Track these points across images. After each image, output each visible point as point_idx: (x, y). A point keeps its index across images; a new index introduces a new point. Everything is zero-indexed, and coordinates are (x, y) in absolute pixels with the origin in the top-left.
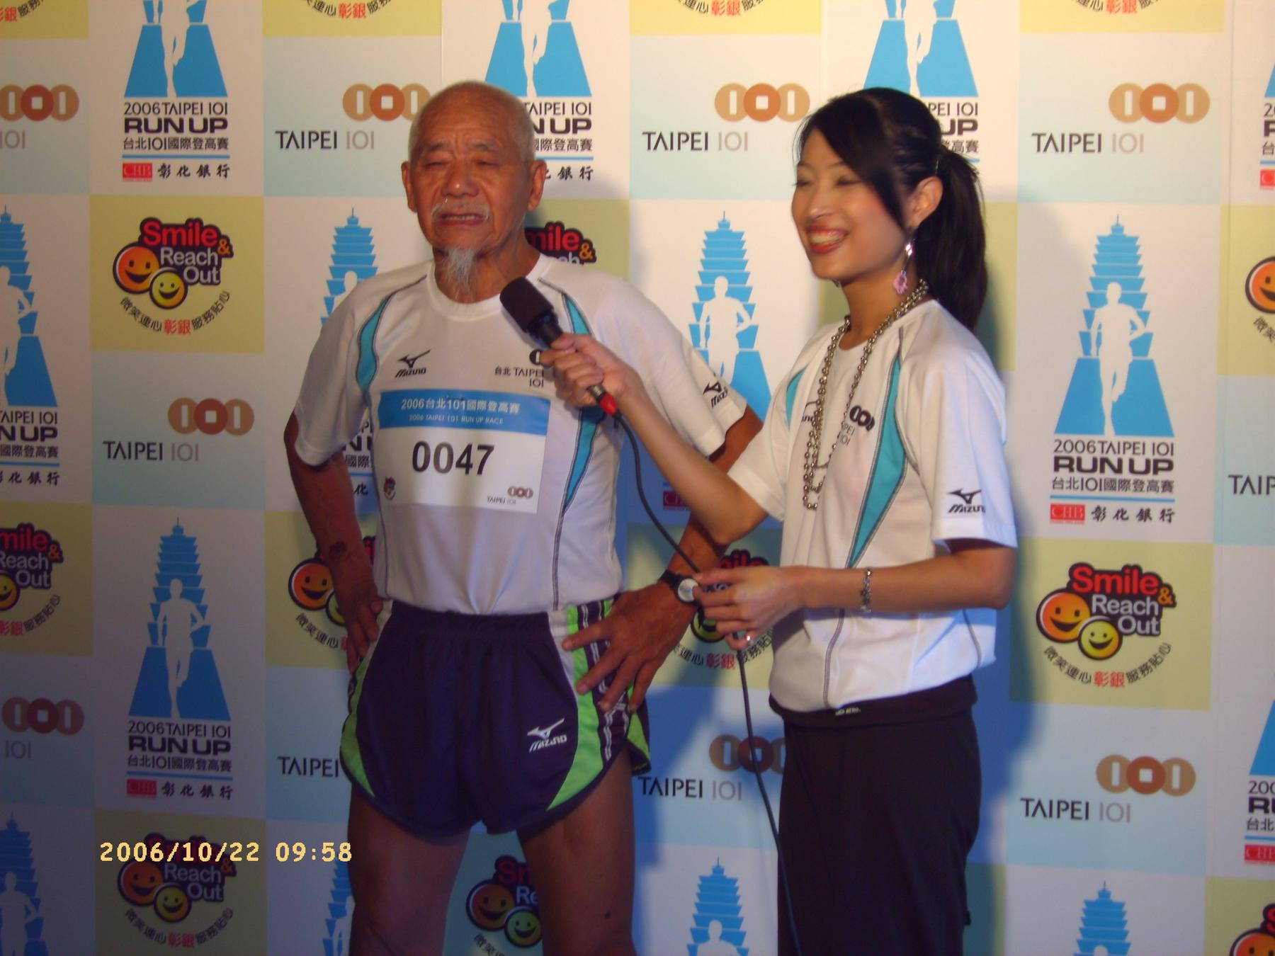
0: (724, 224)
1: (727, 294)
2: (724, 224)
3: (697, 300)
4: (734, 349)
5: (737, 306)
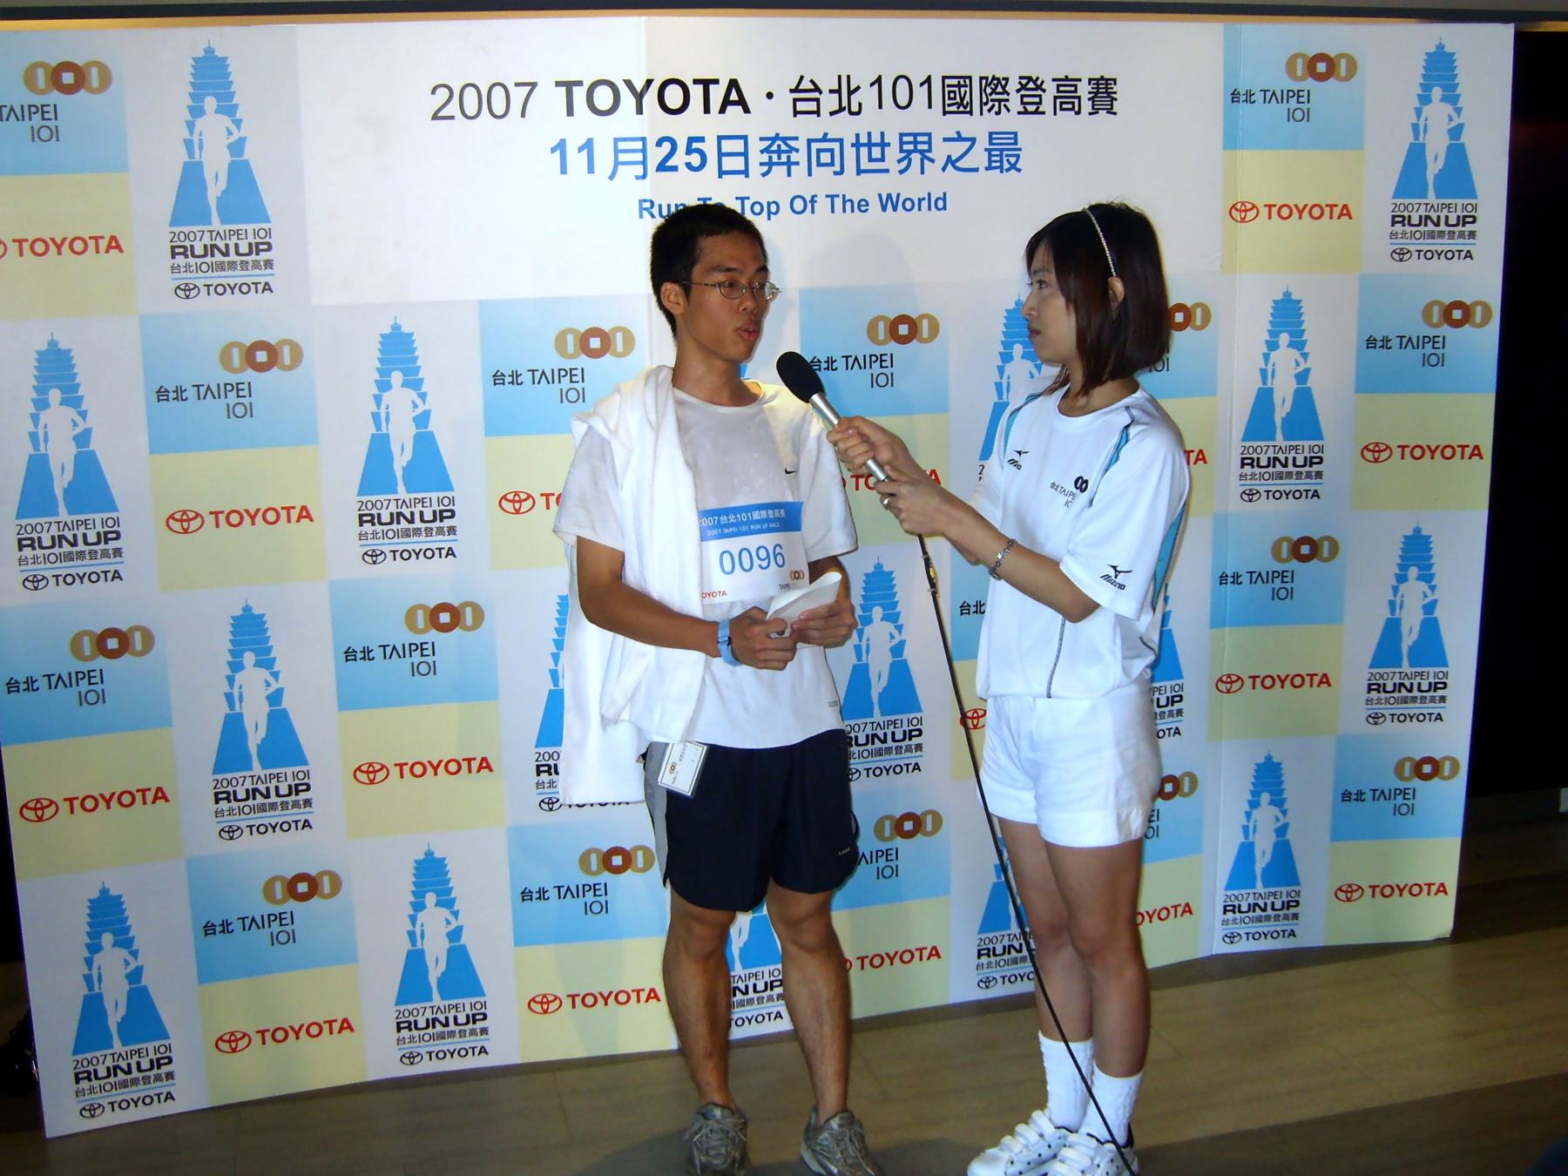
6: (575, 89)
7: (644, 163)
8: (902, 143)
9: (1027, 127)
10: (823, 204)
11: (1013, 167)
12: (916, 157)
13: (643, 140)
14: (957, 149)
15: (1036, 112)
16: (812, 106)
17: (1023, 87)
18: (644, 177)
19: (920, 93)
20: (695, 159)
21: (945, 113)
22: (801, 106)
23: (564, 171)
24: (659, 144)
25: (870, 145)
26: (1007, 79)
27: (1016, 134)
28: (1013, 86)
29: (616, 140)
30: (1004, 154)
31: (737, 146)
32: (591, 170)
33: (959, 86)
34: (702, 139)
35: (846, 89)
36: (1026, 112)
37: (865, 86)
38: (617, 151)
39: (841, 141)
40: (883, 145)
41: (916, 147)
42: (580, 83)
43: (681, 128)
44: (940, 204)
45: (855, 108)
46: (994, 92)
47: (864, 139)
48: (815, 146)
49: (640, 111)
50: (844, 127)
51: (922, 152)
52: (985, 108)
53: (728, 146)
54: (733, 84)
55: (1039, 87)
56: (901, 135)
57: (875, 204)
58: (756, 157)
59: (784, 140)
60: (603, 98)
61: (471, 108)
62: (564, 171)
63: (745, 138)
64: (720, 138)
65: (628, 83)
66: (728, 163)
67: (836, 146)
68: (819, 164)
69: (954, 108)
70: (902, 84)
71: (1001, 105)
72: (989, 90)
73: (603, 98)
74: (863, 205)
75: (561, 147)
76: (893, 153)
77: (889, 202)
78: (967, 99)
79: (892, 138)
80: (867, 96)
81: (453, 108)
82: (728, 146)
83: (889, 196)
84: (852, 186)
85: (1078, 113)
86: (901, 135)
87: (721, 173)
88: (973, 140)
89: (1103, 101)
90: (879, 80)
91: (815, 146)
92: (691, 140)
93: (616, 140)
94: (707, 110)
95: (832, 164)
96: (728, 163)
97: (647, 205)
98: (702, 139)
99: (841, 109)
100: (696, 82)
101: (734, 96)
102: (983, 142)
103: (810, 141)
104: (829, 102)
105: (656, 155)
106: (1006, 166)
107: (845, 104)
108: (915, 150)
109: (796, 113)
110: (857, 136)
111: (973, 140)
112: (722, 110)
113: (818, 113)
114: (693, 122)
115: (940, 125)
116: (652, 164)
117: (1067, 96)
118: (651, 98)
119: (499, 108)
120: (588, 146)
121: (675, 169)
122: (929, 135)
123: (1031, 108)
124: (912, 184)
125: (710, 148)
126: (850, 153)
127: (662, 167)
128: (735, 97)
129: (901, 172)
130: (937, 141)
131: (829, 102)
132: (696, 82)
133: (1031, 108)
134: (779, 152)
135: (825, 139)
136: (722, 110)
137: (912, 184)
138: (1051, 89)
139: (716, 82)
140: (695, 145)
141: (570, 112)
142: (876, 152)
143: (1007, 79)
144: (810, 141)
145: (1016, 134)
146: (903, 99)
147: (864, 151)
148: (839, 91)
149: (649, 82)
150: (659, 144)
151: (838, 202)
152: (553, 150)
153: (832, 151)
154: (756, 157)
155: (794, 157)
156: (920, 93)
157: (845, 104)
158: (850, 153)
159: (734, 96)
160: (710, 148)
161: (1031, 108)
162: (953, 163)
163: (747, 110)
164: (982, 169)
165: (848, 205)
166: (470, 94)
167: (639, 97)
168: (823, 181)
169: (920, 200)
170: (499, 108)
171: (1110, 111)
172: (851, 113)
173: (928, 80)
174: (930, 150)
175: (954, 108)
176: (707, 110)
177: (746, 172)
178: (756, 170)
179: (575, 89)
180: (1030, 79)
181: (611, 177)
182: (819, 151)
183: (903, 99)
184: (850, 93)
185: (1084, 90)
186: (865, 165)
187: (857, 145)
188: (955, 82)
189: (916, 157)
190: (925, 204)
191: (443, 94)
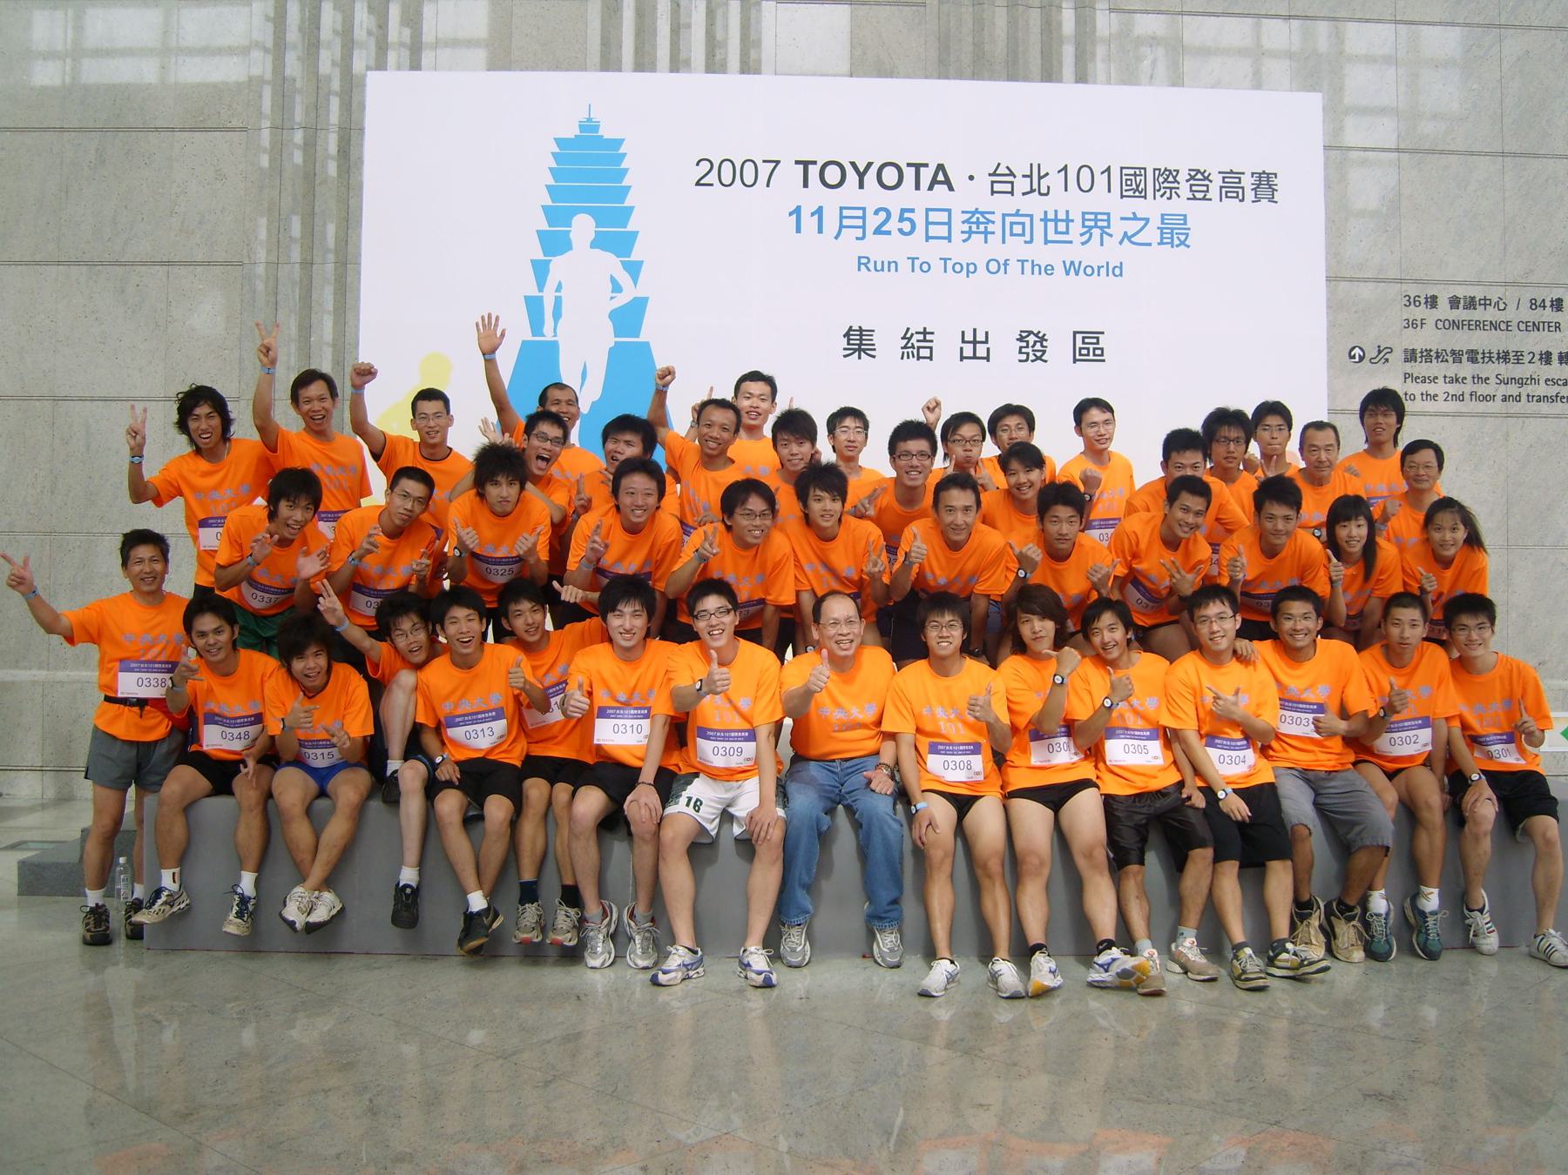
0: (589, 126)
1: (595, 244)
2: (589, 126)
3: (540, 256)
4: (607, 338)
5: (610, 263)
7: (863, 227)
8: (1084, 220)
9: (1195, 210)
10: (1014, 267)
11: (1182, 243)
12: (1096, 232)
13: (864, 209)
14: (1132, 227)
15: (1204, 198)
16: (1008, 187)
17: (1192, 178)
18: (863, 238)
19: (1101, 180)
20: (906, 226)
22: (997, 187)
23: (798, 231)
24: (876, 213)
25: (1056, 220)
30: (1174, 233)
31: (944, 217)
32: (820, 231)
34: (912, 211)
35: (1036, 176)
36: (1195, 198)
38: (842, 217)
39: (1031, 216)
40: (1068, 221)
41: (1096, 224)
42: (815, 163)
46: (1166, 180)
47: (1051, 216)
48: (1008, 220)
49: (861, 186)
50: (1035, 205)
53: (933, 217)
54: (941, 167)
55: (1206, 178)
57: (1059, 269)
58: (958, 226)
59: (982, 214)
60: (833, 175)
61: (727, 179)
62: (798, 231)
63: (949, 211)
64: (928, 210)
65: (853, 164)
66: (933, 231)
68: (1012, 234)
70: (1085, 173)
71: (1172, 192)
73: (833, 175)
74: (1049, 270)
75: (797, 211)
76: (1076, 228)
77: (1071, 268)
79: (1076, 216)
82: (933, 217)
84: (1040, 252)
87: (928, 238)
88: (1147, 220)
90: (1065, 168)
92: (903, 211)
94: (917, 187)
95: (1023, 234)
96: (933, 231)
98: (912, 211)
99: (1032, 191)
100: (909, 165)
101: (941, 177)
102: (1155, 222)
103: (1004, 216)
104: (1022, 185)
105: (873, 222)
106: (1176, 242)
107: (1035, 186)
109: (993, 192)
111: (1147, 220)
112: (931, 188)
113: (1012, 193)
116: (870, 228)
117: (1232, 185)
118: (871, 177)
119: (749, 179)
121: (889, 233)
124: (1092, 254)
125: (919, 218)
126: (1039, 227)
127: (878, 231)
128: (942, 177)
131: (1022, 185)
132: (909, 165)
133: (1199, 194)
134: (978, 223)
135: (1017, 214)
136: (931, 188)
137: (1092, 254)
138: (1217, 181)
139: (926, 165)
140: (906, 215)
141: (806, 185)
142: (1062, 227)
144: (1004, 216)
146: (1086, 185)
147: (1051, 225)
148: (1031, 176)
149: (870, 164)
150: (876, 213)
151: (1028, 266)
153: (1023, 224)
154: (958, 226)
155: (991, 228)
156: (1101, 180)
157: (1035, 186)
158: (1039, 227)
159: (941, 177)
160: (919, 218)
163: (951, 188)
164: (1155, 245)
166: (727, 165)
167: (861, 175)
168: (1015, 248)
170: (749, 179)
171: (1272, 200)
173: (1108, 170)
176: (917, 187)
177: (949, 238)
178: (957, 236)
180: (1198, 171)
181: (836, 238)
182: (1012, 224)
183: (1086, 185)
185: (1248, 182)
186: (1052, 236)
187: (1045, 220)
189: (1096, 232)
190: (1103, 271)
191: (705, 166)
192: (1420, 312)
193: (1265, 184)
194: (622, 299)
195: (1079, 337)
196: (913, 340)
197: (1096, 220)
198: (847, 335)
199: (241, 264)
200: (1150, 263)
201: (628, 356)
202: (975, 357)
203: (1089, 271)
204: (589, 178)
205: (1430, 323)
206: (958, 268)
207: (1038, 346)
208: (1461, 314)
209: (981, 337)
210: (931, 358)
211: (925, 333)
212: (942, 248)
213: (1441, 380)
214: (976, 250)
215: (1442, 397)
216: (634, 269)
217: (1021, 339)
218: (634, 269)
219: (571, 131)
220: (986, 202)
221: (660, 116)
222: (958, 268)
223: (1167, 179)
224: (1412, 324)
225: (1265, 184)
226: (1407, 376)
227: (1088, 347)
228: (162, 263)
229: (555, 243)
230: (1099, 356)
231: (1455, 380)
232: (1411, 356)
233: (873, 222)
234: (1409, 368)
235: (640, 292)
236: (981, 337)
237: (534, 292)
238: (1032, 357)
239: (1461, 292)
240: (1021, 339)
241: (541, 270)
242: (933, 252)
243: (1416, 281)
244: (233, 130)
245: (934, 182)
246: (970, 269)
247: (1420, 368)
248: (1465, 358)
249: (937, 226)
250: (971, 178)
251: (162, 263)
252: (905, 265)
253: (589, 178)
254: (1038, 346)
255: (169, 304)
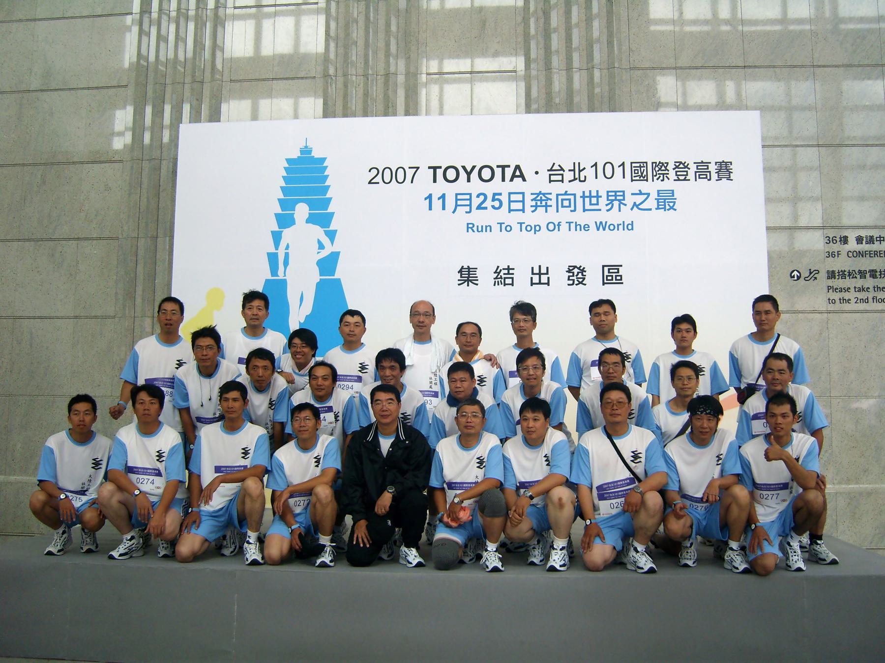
0: (306, 151)
1: (307, 222)
2: (306, 151)
3: (276, 229)
4: (315, 276)
5: (318, 232)
6: (438, 170)
7: (470, 205)
8: (608, 196)
9: (679, 188)
10: (564, 226)
11: (672, 208)
12: (616, 203)
13: (470, 194)
15: (685, 180)
16: (560, 178)
17: (677, 167)
19: (619, 171)
20: (497, 204)
21: (632, 180)
22: (553, 178)
23: (430, 209)
24: (478, 196)
25: (590, 197)
26: (667, 163)
27: (673, 191)
28: (671, 167)
29: (457, 195)
30: (666, 201)
31: (520, 197)
32: (444, 208)
33: (640, 167)
34: (500, 194)
36: (679, 180)
37: (588, 168)
38: (457, 200)
39: (575, 195)
40: (598, 197)
41: (616, 198)
42: (440, 167)
43: (489, 189)
44: (630, 227)
45: (582, 178)
46: (660, 169)
47: (587, 194)
48: (560, 198)
49: (469, 180)
50: (577, 188)
51: (619, 200)
52: (655, 178)
54: (518, 167)
55: (686, 167)
56: (608, 192)
57: (593, 227)
58: (529, 203)
59: (544, 194)
60: (451, 174)
61: (387, 179)
62: (430, 209)
63: (523, 193)
64: (510, 194)
65: (464, 167)
66: (514, 206)
67: (572, 197)
68: (563, 206)
69: (638, 178)
70: (608, 166)
71: (664, 176)
72: (657, 169)
73: (451, 174)
74: (586, 227)
75: (430, 197)
76: (603, 201)
77: (601, 226)
78: (645, 173)
79: (603, 194)
80: (589, 173)
81: (379, 179)
83: (601, 223)
84: (581, 217)
85: (710, 180)
86: (608, 192)
87: (510, 211)
88: (648, 194)
89: (724, 173)
90: (596, 165)
91: (560, 198)
92: (495, 194)
93: (457, 195)
94: (503, 180)
95: (570, 206)
96: (514, 206)
97: (470, 226)
98: (500, 194)
99: (575, 179)
100: (498, 166)
101: (518, 173)
102: (654, 195)
103: (557, 195)
104: (568, 176)
105: (476, 202)
106: (668, 207)
107: (577, 176)
108: (616, 200)
109: (550, 181)
110: (584, 192)
111: (648, 194)
112: (512, 180)
113: (562, 181)
114: (496, 185)
115: (629, 186)
117: (703, 170)
118: (474, 175)
119: (400, 179)
120: (443, 197)
121: (486, 208)
122: (624, 192)
123: (682, 178)
124: (614, 217)
126: (579, 201)
127: (479, 207)
128: (519, 173)
129: (608, 210)
130: (628, 195)
131: (568, 176)
132: (498, 166)
134: (541, 200)
135: (566, 194)
136: (512, 180)
137: (614, 217)
138: (693, 168)
139: (509, 166)
140: (496, 197)
141: (435, 181)
142: (594, 201)
143: (667, 163)
144: (557, 195)
145: (673, 191)
146: (609, 175)
147: (587, 200)
148: (574, 170)
149: (474, 167)
150: (478, 196)
151: (573, 226)
152: (426, 199)
154: (529, 203)
155: (549, 203)
156: (619, 171)
157: (577, 176)
158: (579, 201)
159: (518, 173)
160: (504, 199)
161: (682, 178)
162: (637, 206)
163: (524, 180)
165: (578, 227)
166: (387, 172)
167: (469, 174)
168: (565, 215)
169: (618, 225)
170: (400, 179)
171: (729, 179)
172: (580, 181)
173: (623, 164)
174: (624, 199)
175: (638, 178)
176: (503, 180)
177: (523, 210)
178: (528, 208)
179: (438, 170)
180: (681, 163)
181: (454, 212)
182: (562, 200)
183: (609, 175)
184: (580, 171)
185: (713, 168)
186: (587, 206)
187: (584, 197)
188: (638, 165)
189: (616, 203)
190: (621, 227)
191: (374, 172)
192: (836, 247)
193: (725, 169)
194: (324, 253)
195: (606, 269)
196: (501, 274)
197: (616, 196)
198: (460, 271)
199: (117, 238)
200: (651, 221)
201: (329, 288)
202: (540, 283)
203: (612, 227)
204: (306, 181)
205: (844, 254)
206: (529, 228)
207: (580, 275)
208: (864, 247)
209: (544, 271)
210: (512, 284)
211: (508, 269)
212: (518, 217)
213: (852, 290)
214: (540, 217)
215: (853, 300)
216: (331, 235)
217: (569, 271)
218: (331, 235)
219: (296, 154)
220: (546, 187)
221: (352, 144)
222: (529, 228)
223: (660, 168)
224: (831, 255)
225: (725, 169)
226: (829, 288)
227: (612, 274)
228: (74, 239)
229: (285, 220)
230: (619, 281)
231: (862, 289)
232: (831, 275)
233: (476, 202)
234: (831, 282)
235: (335, 249)
236: (544, 271)
237: (273, 250)
238: (576, 282)
239: (864, 233)
240: (569, 271)
241: (277, 237)
242: (513, 219)
243: (833, 227)
244: (115, 162)
245: (514, 176)
246: (536, 229)
247: (838, 283)
248: (868, 275)
249: (516, 203)
250: (537, 173)
251: (74, 239)
252: (496, 228)
253: (306, 181)
254: (580, 275)
255: (78, 263)
